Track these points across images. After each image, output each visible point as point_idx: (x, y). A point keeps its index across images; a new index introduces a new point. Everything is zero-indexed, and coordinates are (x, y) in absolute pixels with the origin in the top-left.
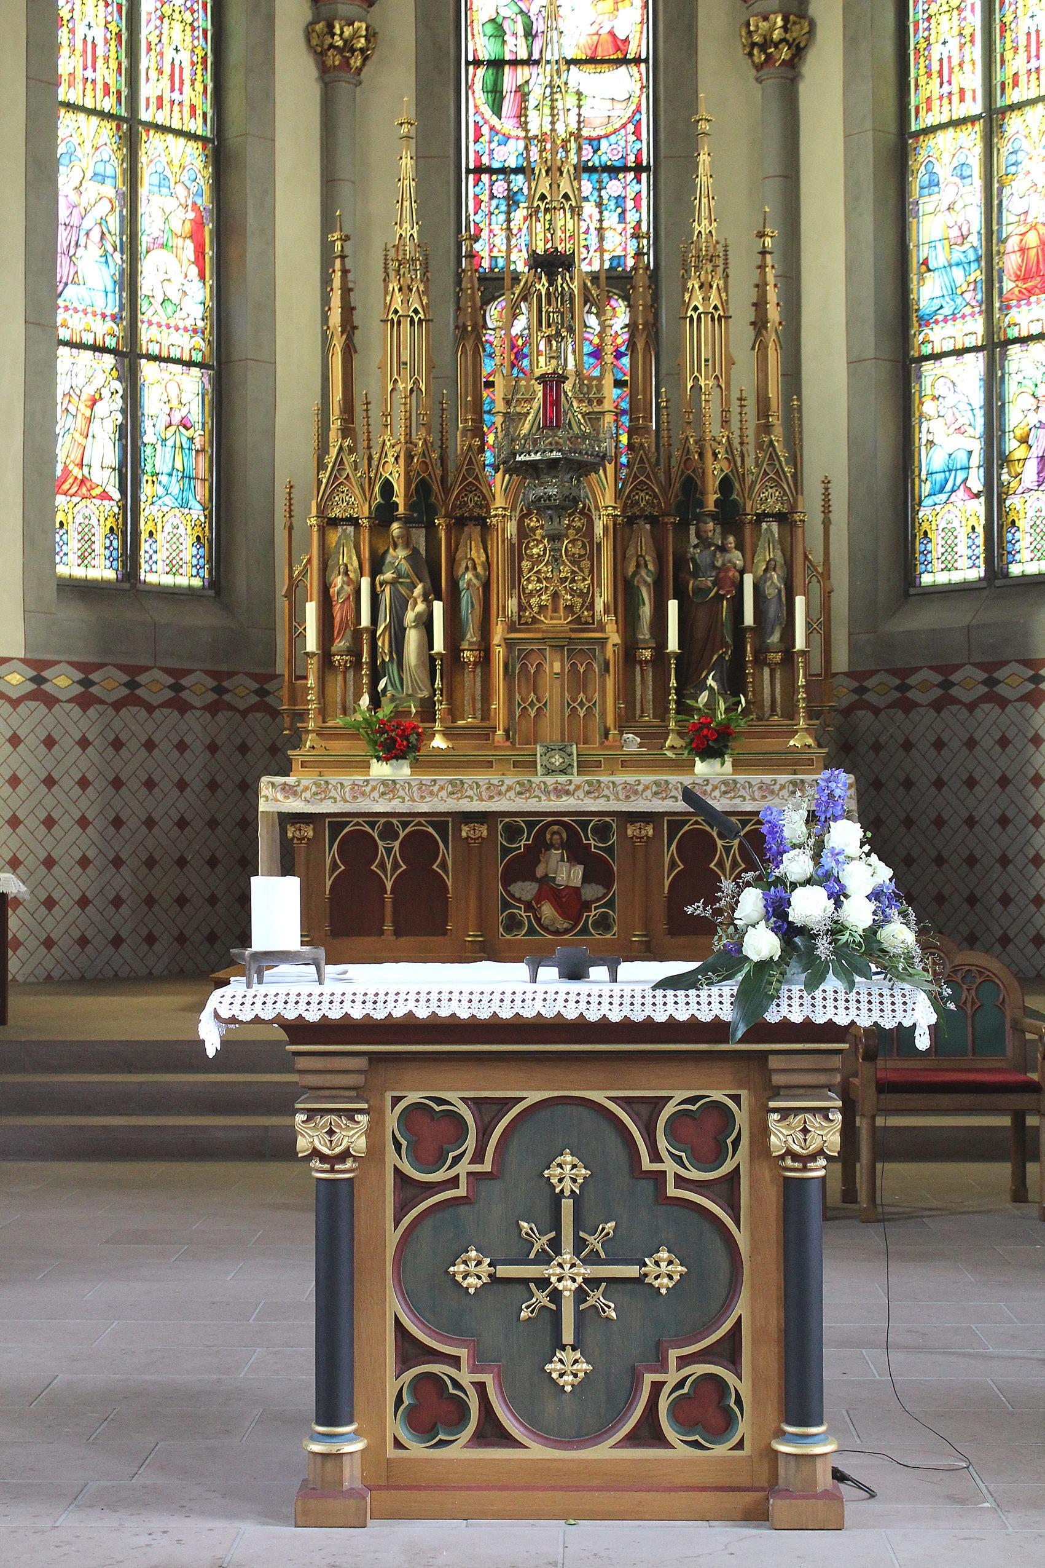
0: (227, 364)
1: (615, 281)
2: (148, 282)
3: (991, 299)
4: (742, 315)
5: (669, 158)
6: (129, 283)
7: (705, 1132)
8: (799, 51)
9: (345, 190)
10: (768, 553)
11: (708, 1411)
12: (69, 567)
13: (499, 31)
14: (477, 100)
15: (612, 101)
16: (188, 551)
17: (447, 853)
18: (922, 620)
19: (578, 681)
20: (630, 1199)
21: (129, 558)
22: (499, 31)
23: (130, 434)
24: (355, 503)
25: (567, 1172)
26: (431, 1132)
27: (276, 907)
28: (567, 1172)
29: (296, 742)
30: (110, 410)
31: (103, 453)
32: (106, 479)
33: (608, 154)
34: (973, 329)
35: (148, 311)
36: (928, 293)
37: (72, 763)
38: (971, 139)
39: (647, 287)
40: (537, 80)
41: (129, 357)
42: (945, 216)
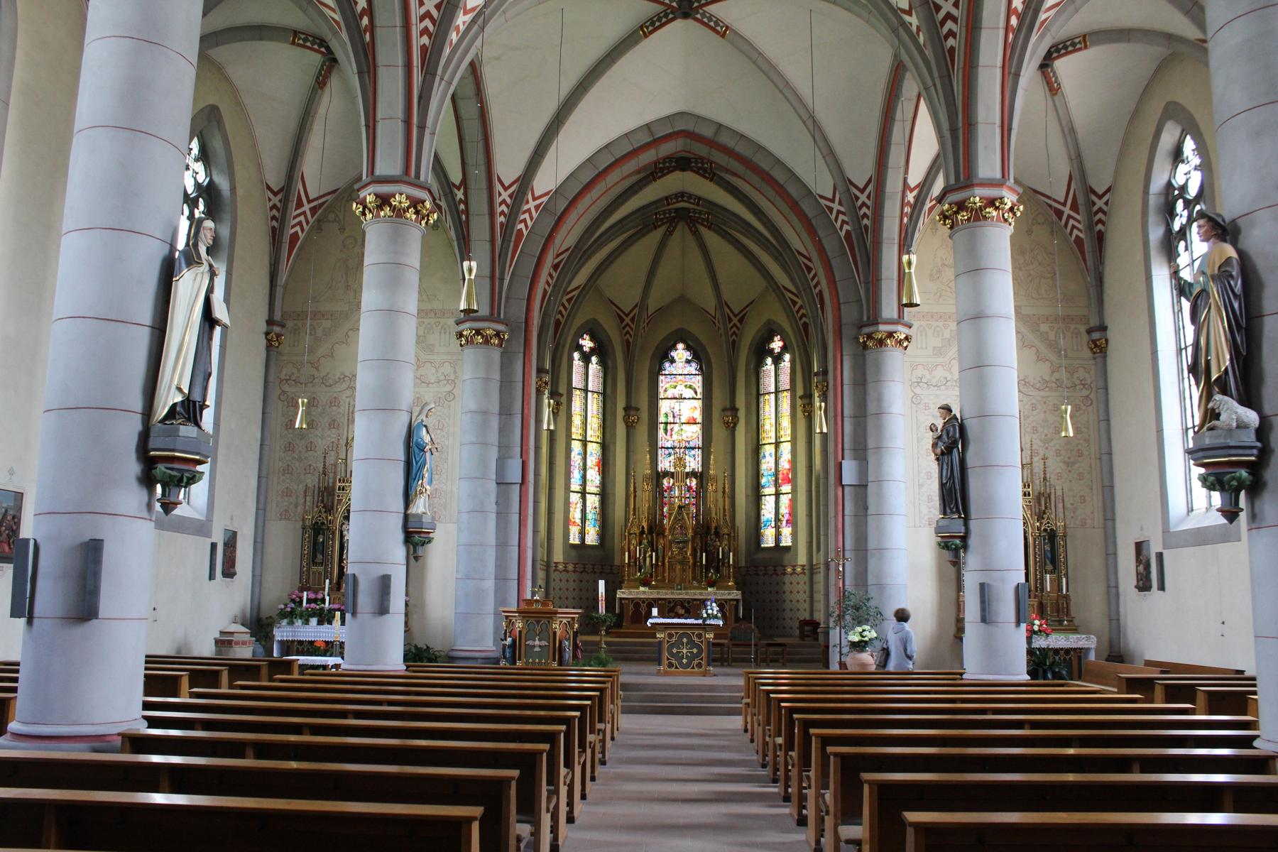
0: (604, 494)
1: (693, 474)
2: (588, 476)
3: (777, 484)
4: (720, 490)
5: (706, 448)
6: (584, 477)
7: (699, 636)
8: (735, 424)
10: (726, 542)
11: (699, 665)
12: (571, 541)
13: (667, 415)
14: (661, 432)
15: (693, 433)
18: (760, 555)
19: (684, 570)
20: (691, 643)
21: (583, 538)
22: (667, 415)
24: (635, 530)
26: (670, 636)
27: (655, 611)
29: (622, 582)
30: (580, 506)
32: (578, 521)
33: (692, 444)
34: (772, 490)
35: (588, 483)
36: (763, 481)
37: (572, 585)
38: (773, 447)
39: (700, 476)
40: (676, 427)
41: (583, 494)
42: (767, 464)
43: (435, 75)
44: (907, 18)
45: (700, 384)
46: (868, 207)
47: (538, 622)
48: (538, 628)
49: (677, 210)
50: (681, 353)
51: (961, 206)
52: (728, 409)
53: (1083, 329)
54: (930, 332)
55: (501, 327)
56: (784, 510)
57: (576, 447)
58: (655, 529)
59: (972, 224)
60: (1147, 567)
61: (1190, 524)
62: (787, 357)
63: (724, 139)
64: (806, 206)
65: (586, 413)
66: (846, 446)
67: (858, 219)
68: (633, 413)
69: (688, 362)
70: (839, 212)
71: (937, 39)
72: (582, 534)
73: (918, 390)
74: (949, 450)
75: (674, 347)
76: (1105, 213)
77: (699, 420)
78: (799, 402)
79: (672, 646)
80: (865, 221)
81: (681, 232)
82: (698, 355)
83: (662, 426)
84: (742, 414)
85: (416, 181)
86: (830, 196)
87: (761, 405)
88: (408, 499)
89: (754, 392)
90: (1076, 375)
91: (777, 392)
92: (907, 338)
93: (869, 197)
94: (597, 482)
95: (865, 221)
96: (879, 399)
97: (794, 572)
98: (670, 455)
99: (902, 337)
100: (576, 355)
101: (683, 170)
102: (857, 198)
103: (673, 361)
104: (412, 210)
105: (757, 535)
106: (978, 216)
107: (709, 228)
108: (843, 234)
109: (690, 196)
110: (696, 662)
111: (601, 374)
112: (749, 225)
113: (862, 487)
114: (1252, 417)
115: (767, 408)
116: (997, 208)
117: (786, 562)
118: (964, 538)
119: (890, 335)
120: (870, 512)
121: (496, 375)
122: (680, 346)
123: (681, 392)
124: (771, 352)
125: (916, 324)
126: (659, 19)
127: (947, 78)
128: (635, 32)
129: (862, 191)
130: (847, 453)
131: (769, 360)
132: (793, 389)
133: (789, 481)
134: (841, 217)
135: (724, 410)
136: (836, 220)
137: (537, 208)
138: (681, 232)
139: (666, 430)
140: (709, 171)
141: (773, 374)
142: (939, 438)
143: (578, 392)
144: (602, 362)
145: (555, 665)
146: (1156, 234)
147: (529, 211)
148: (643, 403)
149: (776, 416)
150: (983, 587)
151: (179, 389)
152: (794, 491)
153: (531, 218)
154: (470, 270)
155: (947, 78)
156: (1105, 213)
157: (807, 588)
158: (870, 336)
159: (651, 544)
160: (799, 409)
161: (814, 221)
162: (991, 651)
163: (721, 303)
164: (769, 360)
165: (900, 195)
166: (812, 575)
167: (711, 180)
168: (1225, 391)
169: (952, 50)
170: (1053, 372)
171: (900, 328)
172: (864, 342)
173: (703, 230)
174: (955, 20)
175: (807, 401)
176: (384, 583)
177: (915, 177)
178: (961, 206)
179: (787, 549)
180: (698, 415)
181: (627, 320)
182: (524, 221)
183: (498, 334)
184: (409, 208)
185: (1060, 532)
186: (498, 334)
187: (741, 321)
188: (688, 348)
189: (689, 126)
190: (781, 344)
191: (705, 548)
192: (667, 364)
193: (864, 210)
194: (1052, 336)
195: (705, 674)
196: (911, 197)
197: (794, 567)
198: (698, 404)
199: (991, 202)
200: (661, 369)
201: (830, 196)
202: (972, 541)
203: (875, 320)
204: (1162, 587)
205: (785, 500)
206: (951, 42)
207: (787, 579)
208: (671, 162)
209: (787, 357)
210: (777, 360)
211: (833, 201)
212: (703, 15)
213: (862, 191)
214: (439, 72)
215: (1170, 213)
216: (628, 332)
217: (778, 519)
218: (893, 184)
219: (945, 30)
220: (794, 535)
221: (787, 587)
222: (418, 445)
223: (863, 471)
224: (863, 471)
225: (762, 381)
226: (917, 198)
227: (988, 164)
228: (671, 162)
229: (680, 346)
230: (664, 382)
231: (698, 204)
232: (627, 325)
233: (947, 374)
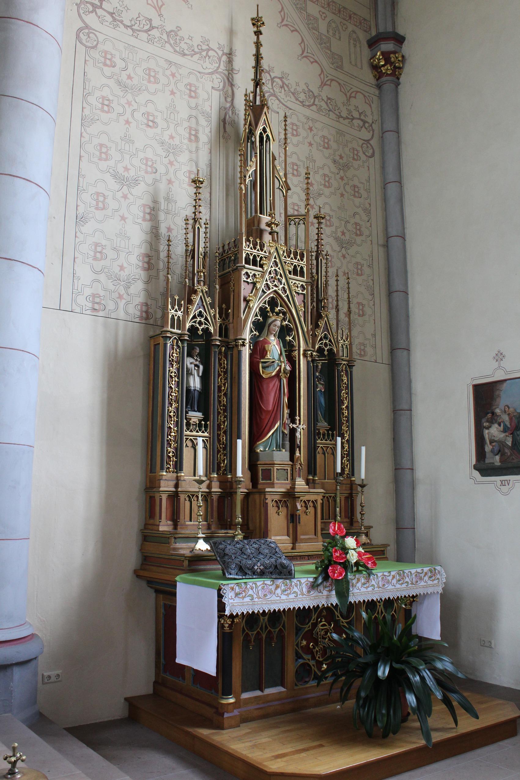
53: (363, 37)
73: (91, 20)
90: (353, 101)
170: (323, 84)
185: (343, 354)
194: (323, 27)
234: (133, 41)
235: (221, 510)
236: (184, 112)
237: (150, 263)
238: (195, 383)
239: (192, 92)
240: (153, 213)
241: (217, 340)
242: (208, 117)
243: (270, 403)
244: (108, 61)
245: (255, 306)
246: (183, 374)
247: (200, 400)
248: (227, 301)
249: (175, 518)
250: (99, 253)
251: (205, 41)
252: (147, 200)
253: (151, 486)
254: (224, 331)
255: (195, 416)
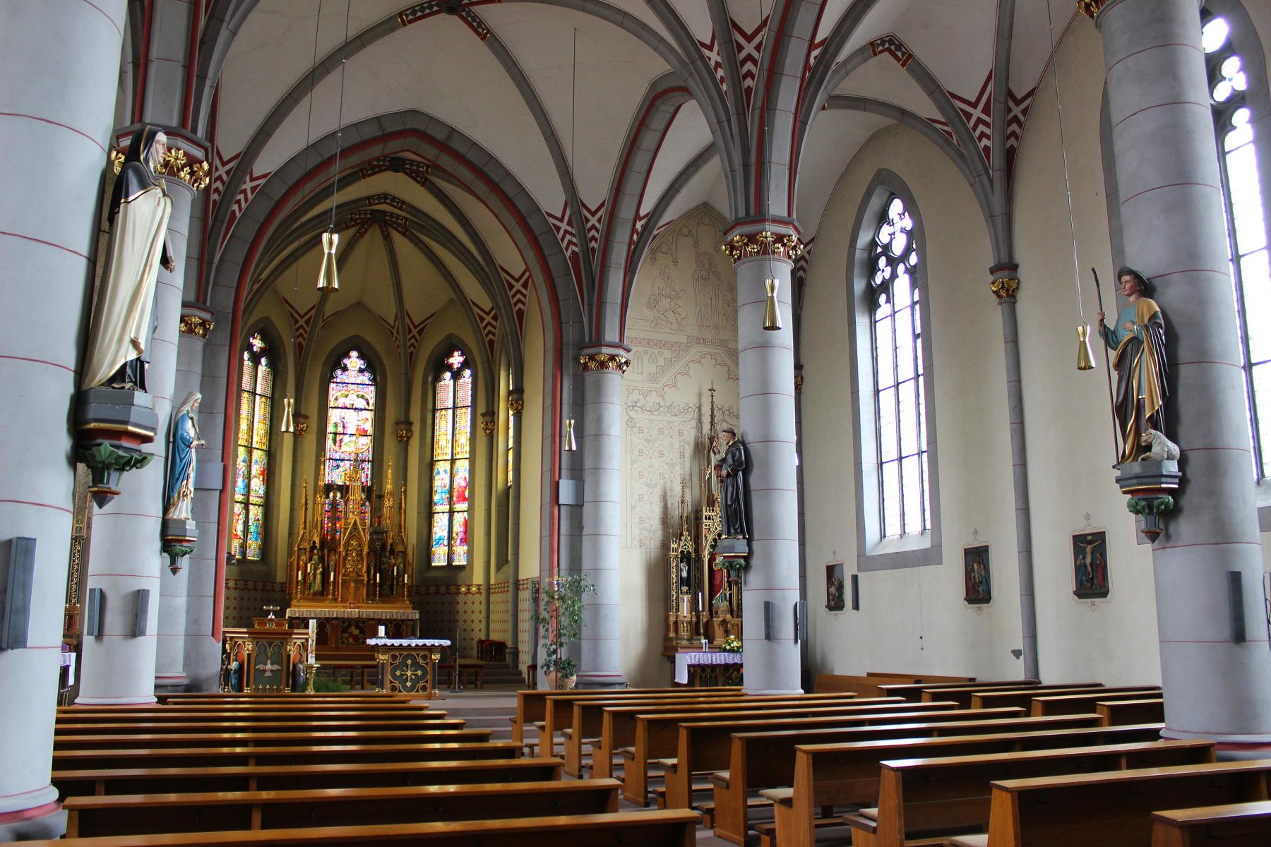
0: (268, 505)
4: (397, 506)
5: (377, 461)
6: (248, 486)
7: (424, 657)
8: (409, 438)
9: (299, 464)
11: (424, 688)
13: (336, 425)
14: (329, 443)
16: (257, 551)
17: (328, 627)
18: (433, 574)
19: (357, 588)
20: (416, 665)
21: (244, 553)
23: (246, 523)
24: (306, 545)
25: (409, 662)
26: (394, 657)
27: (382, 630)
28: (409, 662)
29: (291, 599)
31: (240, 527)
34: (447, 508)
36: (436, 498)
38: (447, 465)
40: (346, 438)
41: (246, 504)
42: (441, 480)
43: (222, 20)
44: (706, 52)
45: (373, 395)
46: (597, 231)
47: (270, 644)
48: (270, 651)
49: (373, 211)
50: (354, 362)
51: (752, 238)
52: (402, 424)
54: (645, 358)
55: (207, 316)
56: (458, 527)
57: (242, 453)
58: (328, 545)
59: (761, 257)
60: (840, 587)
61: (889, 548)
62: (467, 373)
63: (456, 144)
64: (533, 222)
65: (253, 419)
66: (564, 466)
67: (585, 241)
68: (301, 420)
69: (361, 371)
70: (566, 232)
71: (737, 78)
72: (244, 547)
73: (633, 414)
74: (732, 475)
75: (347, 355)
76: (806, 261)
77: (370, 431)
78: (480, 419)
79: (395, 668)
80: (593, 244)
81: (374, 234)
82: (372, 365)
83: (330, 437)
84: (416, 428)
85: (192, 136)
86: (559, 216)
87: (437, 421)
88: (167, 506)
89: (430, 406)
91: (455, 408)
92: (627, 363)
93: (599, 221)
94: (261, 493)
95: (593, 244)
96: (599, 420)
97: (468, 592)
98: (338, 467)
99: (623, 360)
100: (246, 356)
101: (396, 171)
102: (587, 220)
103: (345, 369)
104: (187, 169)
105: (428, 555)
106: (765, 250)
107: (404, 234)
108: (568, 254)
109: (394, 199)
110: (421, 684)
111: (270, 377)
112: (453, 236)
113: (577, 508)
114: (1175, 449)
115: (443, 423)
116: (784, 245)
117: (460, 582)
118: (747, 559)
119: (612, 358)
120: (585, 532)
121: (198, 369)
122: (354, 354)
123: (351, 402)
124: (449, 367)
125: (634, 349)
126: (422, 10)
127: (742, 115)
128: (393, 18)
129: (593, 214)
130: (564, 472)
131: (448, 375)
132: (474, 405)
133: (465, 499)
134: (568, 237)
135: (397, 423)
136: (563, 239)
137: (253, 189)
138: (374, 234)
139: (335, 441)
140: (420, 175)
141: (451, 389)
142: (724, 460)
143: (245, 395)
144: (271, 365)
145: (288, 691)
146: (859, 286)
147: (244, 191)
148: (312, 410)
149: (453, 431)
150: (768, 606)
151: (135, 343)
152: (471, 510)
153: (246, 200)
154: (331, 244)
155: (742, 115)
156: (806, 261)
157: (483, 608)
158: (592, 358)
159: (322, 559)
160: (480, 426)
161: (540, 239)
162: (771, 666)
163: (402, 313)
164: (448, 375)
165: (631, 222)
166: (488, 594)
167: (423, 185)
168: (1156, 427)
169: (749, 90)
171: (621, 352)
172: (586, 363)
173: (397, 238)
174: (755, 62)
175: (489, 419)
176: (139, 600)
177: (645, 209)
178: (752, 238)
179: (461, 568)
180: (369, 427)
181: (302, 322)
182: (239, 202)
183: (203, 324)
184: (184, 166)
186: (203, 324)
187: (420, 333)
188: (361, 357)
189: (422, 127)
190: (461, 359)
191: (379, 569)
192: (339, 372)
193: (593, 232)
195: (429, 698)
196: (639, 225)
197: (469, 587)
198: (370, 415)
199: (779, 239)
200: (332, 377)
201: (559, 216)
202: (755, 562)
203: (598, 342)
204: (856, 606)
205: (459, 519)
206: (749, 82)
207: (460, 598)
208: (385, 161)
209: (467, 373)
210: (456, 375)
211: (561, 220)
212: (468, 13)
213: (593, 214)
214: (227, 18)
215: (872, 268)
216: (301, 335)
217: (451, 538)
218: (626, 212)
219: (745, 69)
220: (470, 554)
221: (461, 608)
222: (183, 439)
223: (579, 492)
224: (579, 492)
225: (438, 397)
226: (645, 227)
227: (777, 205)
228: (385, 161)
229: (354, 354)
230: (334, 390)
231: (401, 209)
232: (301, 327)
233: (659, 400)
234: (652, 417)
235: (695, 629)
236: (677, 444)
237: (665, 521)
238: (685, 574)
239: (681, 433)
240: (664, 498)
241: (693, 555)
242: (688, 443)
243: (717, 582)
244: (641, 431)
245: (710, 538)
246: (679, 571)
247: (683, 582)
248: (697, 539)
249: (676, 631)
250: (641, 521)
251: (687, 404)
252: (661, 492)
253: (667, 618)
254: (697, 551)
255: (685, 589)
